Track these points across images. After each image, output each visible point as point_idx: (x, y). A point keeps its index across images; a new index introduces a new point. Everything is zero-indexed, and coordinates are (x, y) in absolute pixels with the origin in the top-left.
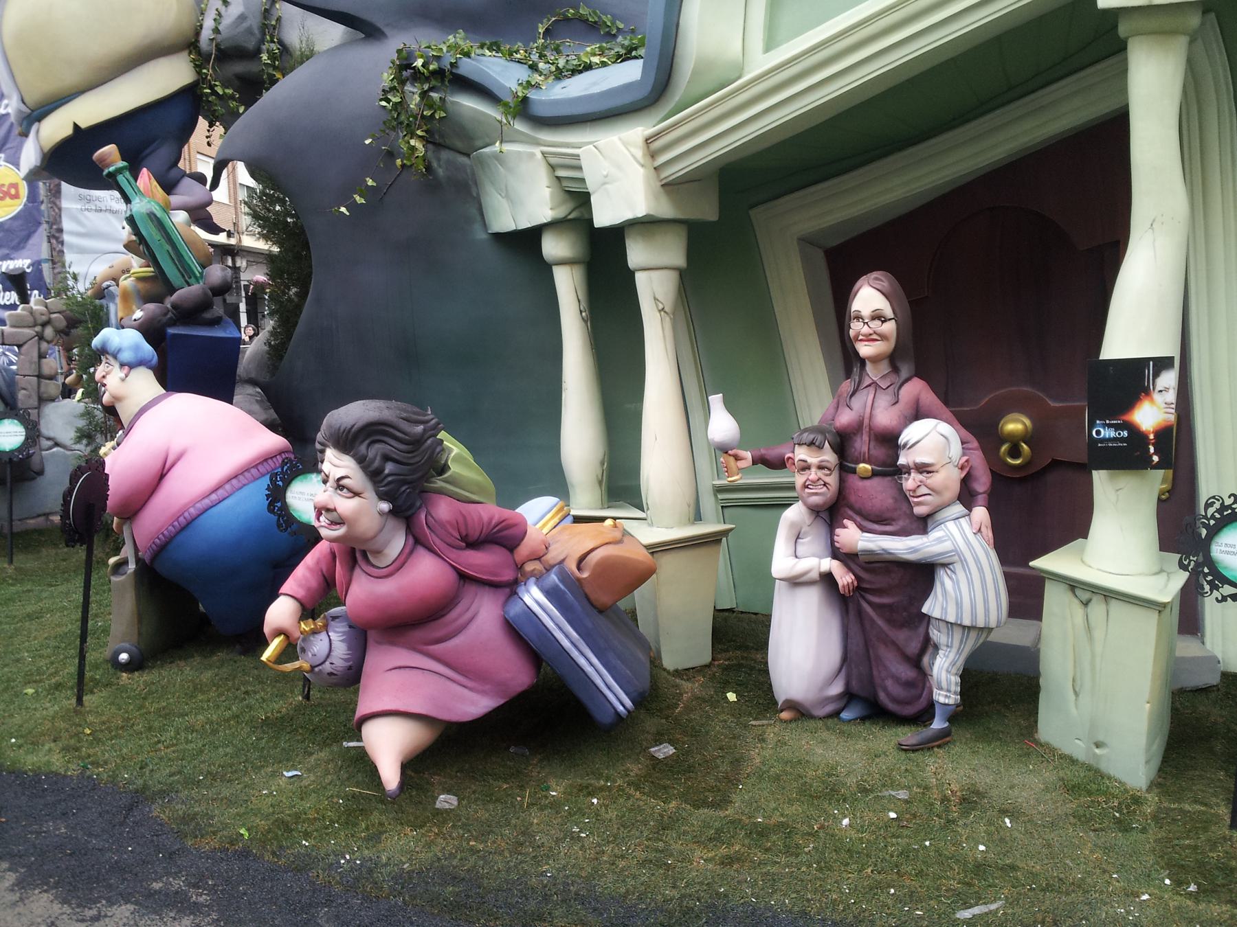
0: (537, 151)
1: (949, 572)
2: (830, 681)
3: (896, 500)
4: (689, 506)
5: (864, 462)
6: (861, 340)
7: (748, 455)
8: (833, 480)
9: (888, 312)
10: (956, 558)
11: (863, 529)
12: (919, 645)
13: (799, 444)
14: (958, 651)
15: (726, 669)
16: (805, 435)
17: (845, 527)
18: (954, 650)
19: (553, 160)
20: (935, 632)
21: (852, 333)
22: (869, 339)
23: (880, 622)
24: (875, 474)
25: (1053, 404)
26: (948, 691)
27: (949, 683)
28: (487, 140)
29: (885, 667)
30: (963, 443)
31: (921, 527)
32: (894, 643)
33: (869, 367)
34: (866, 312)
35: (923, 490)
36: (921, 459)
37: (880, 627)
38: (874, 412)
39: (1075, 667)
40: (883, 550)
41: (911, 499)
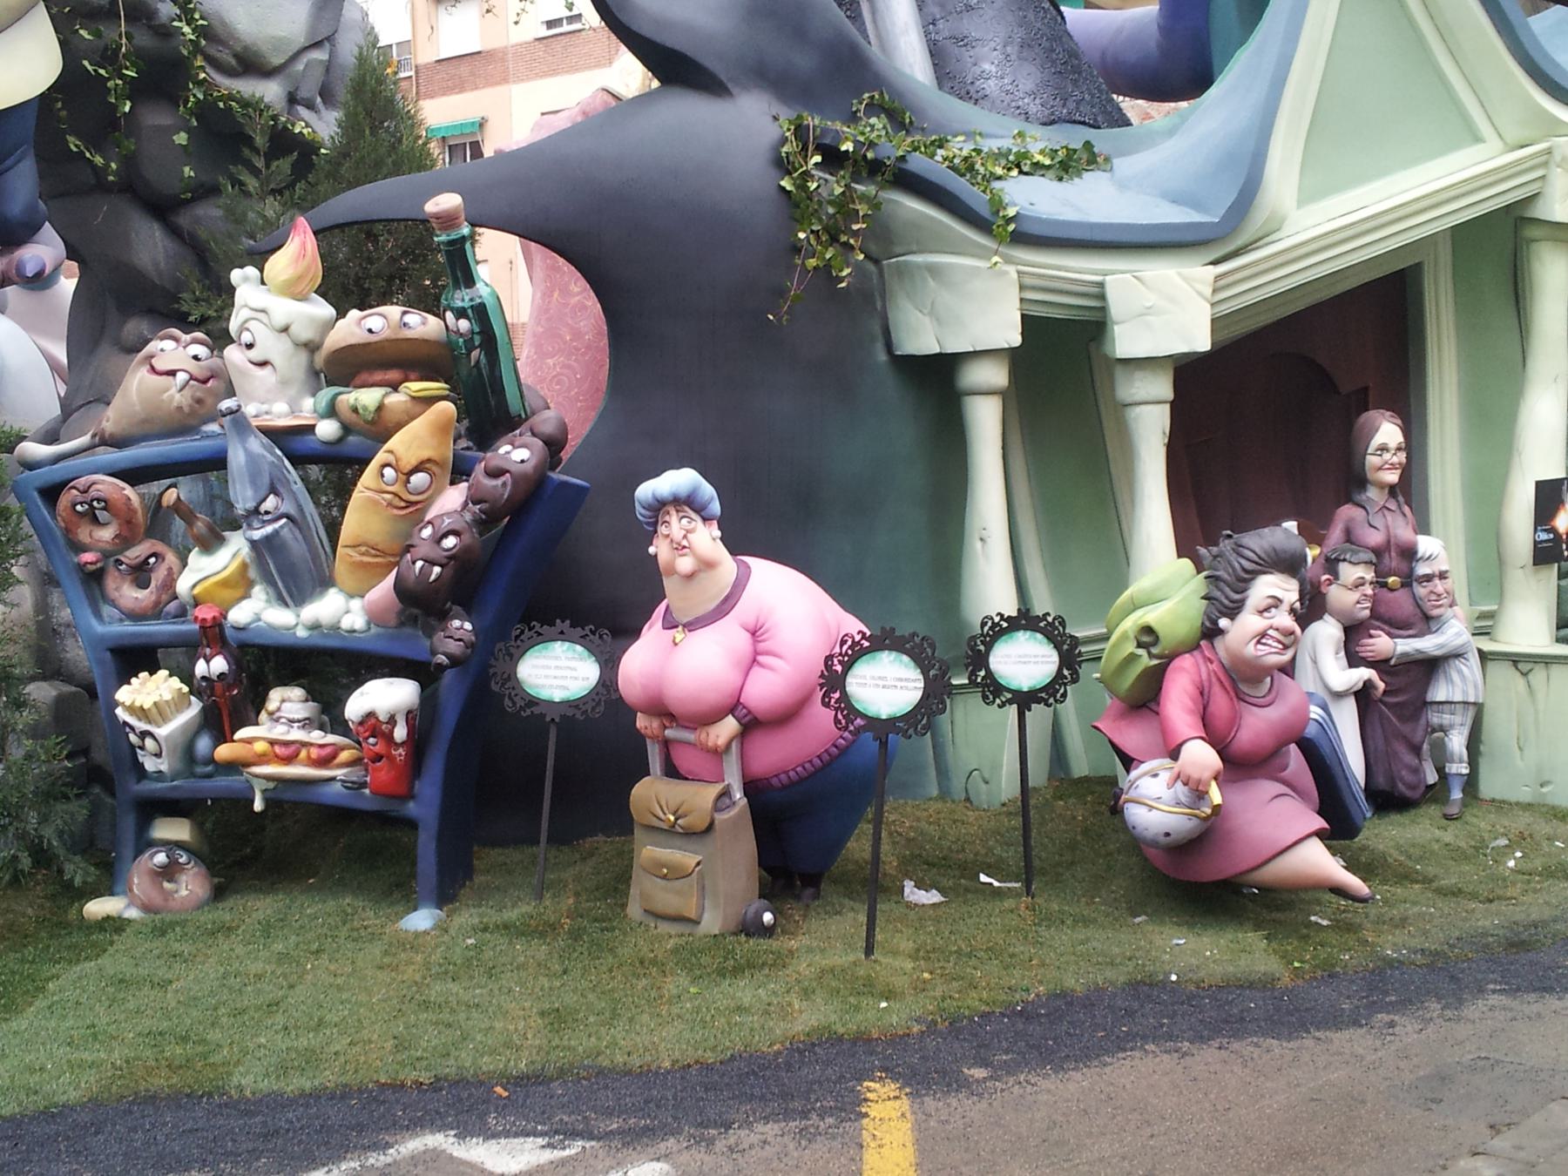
0: (1012, 271)
11: (1392, 636)
17: (1371, 636)
19: (1028, 281)
20: (1448, 716)
24: (1403, 585)
28: (914, 248)
32: (1405, 737)
33: (1372, 493)
39: (1518, 726)
40: (1417, 650)
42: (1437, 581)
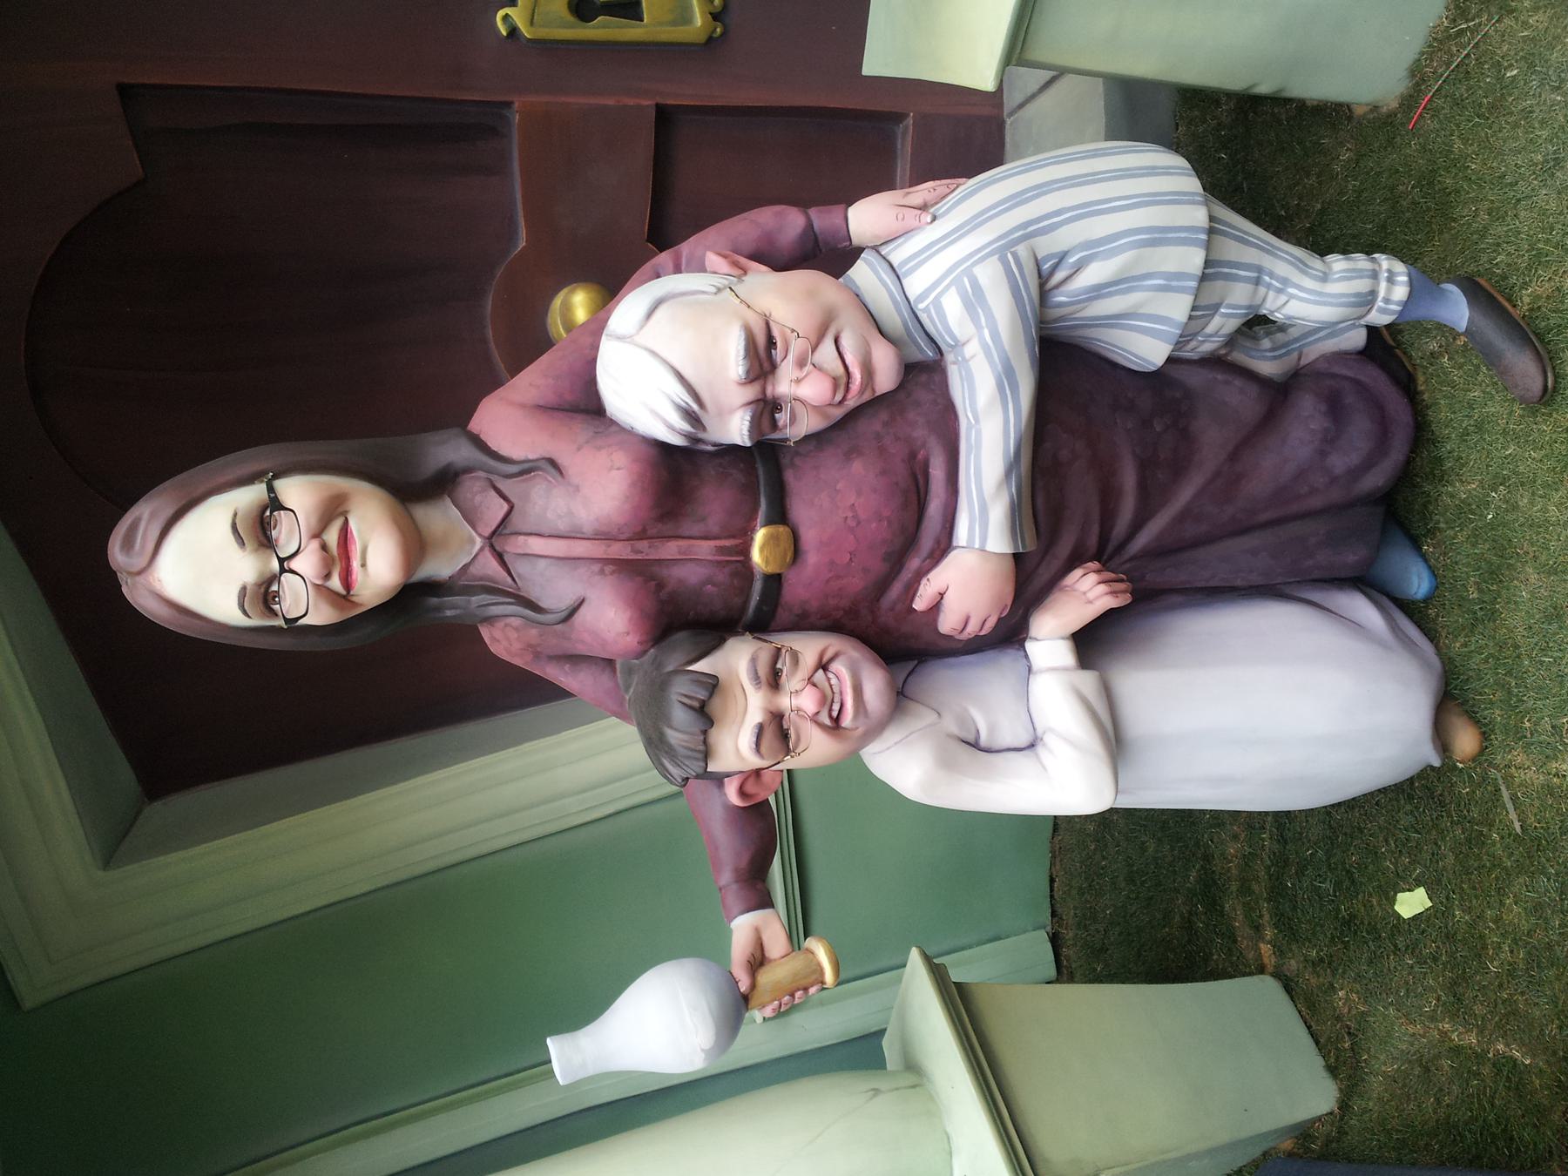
1: (1059, 276)
2: (1356, 627)
3: (849, 456)
4: (877, 1091)
5: (745, 551)
6: (347, 582)
7: (743, 926)
8: (809, 647)
9: (249, 496)
10: (1022, 250)
11: (944, 546)
12: (1238, 382)
13: (706, 754)
14: (1267, 252)
15: (1289, 932)
16: (673, 737)
17: (936, 608)
18: (1267, 262)
21: (320, 615)
22: (340, 558)
23: (1185, 494)
24: (779, 515)
25: (522, 243)
26: (1375, 275)
27: (1358, 274)
29: (1301, 474)
30: (658, 276)
31: (924, 378)
32: (1234, 456)
33: (440, 567)
34: (246, 567)
35: (827, 351)
36: (735, 365)
37: (1198, 495)
38: (588, 529)
40: (1008, 474)
41: (851, 403)
42: (785, 384)
